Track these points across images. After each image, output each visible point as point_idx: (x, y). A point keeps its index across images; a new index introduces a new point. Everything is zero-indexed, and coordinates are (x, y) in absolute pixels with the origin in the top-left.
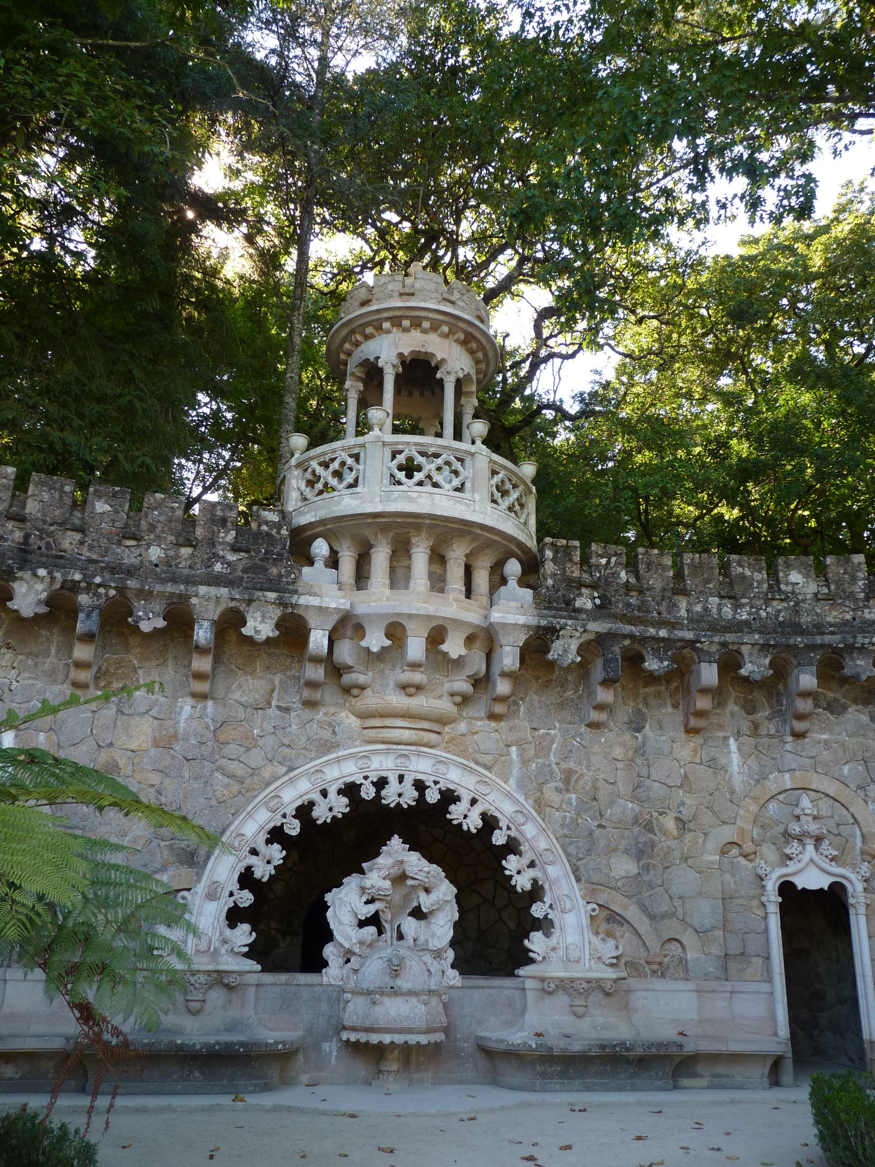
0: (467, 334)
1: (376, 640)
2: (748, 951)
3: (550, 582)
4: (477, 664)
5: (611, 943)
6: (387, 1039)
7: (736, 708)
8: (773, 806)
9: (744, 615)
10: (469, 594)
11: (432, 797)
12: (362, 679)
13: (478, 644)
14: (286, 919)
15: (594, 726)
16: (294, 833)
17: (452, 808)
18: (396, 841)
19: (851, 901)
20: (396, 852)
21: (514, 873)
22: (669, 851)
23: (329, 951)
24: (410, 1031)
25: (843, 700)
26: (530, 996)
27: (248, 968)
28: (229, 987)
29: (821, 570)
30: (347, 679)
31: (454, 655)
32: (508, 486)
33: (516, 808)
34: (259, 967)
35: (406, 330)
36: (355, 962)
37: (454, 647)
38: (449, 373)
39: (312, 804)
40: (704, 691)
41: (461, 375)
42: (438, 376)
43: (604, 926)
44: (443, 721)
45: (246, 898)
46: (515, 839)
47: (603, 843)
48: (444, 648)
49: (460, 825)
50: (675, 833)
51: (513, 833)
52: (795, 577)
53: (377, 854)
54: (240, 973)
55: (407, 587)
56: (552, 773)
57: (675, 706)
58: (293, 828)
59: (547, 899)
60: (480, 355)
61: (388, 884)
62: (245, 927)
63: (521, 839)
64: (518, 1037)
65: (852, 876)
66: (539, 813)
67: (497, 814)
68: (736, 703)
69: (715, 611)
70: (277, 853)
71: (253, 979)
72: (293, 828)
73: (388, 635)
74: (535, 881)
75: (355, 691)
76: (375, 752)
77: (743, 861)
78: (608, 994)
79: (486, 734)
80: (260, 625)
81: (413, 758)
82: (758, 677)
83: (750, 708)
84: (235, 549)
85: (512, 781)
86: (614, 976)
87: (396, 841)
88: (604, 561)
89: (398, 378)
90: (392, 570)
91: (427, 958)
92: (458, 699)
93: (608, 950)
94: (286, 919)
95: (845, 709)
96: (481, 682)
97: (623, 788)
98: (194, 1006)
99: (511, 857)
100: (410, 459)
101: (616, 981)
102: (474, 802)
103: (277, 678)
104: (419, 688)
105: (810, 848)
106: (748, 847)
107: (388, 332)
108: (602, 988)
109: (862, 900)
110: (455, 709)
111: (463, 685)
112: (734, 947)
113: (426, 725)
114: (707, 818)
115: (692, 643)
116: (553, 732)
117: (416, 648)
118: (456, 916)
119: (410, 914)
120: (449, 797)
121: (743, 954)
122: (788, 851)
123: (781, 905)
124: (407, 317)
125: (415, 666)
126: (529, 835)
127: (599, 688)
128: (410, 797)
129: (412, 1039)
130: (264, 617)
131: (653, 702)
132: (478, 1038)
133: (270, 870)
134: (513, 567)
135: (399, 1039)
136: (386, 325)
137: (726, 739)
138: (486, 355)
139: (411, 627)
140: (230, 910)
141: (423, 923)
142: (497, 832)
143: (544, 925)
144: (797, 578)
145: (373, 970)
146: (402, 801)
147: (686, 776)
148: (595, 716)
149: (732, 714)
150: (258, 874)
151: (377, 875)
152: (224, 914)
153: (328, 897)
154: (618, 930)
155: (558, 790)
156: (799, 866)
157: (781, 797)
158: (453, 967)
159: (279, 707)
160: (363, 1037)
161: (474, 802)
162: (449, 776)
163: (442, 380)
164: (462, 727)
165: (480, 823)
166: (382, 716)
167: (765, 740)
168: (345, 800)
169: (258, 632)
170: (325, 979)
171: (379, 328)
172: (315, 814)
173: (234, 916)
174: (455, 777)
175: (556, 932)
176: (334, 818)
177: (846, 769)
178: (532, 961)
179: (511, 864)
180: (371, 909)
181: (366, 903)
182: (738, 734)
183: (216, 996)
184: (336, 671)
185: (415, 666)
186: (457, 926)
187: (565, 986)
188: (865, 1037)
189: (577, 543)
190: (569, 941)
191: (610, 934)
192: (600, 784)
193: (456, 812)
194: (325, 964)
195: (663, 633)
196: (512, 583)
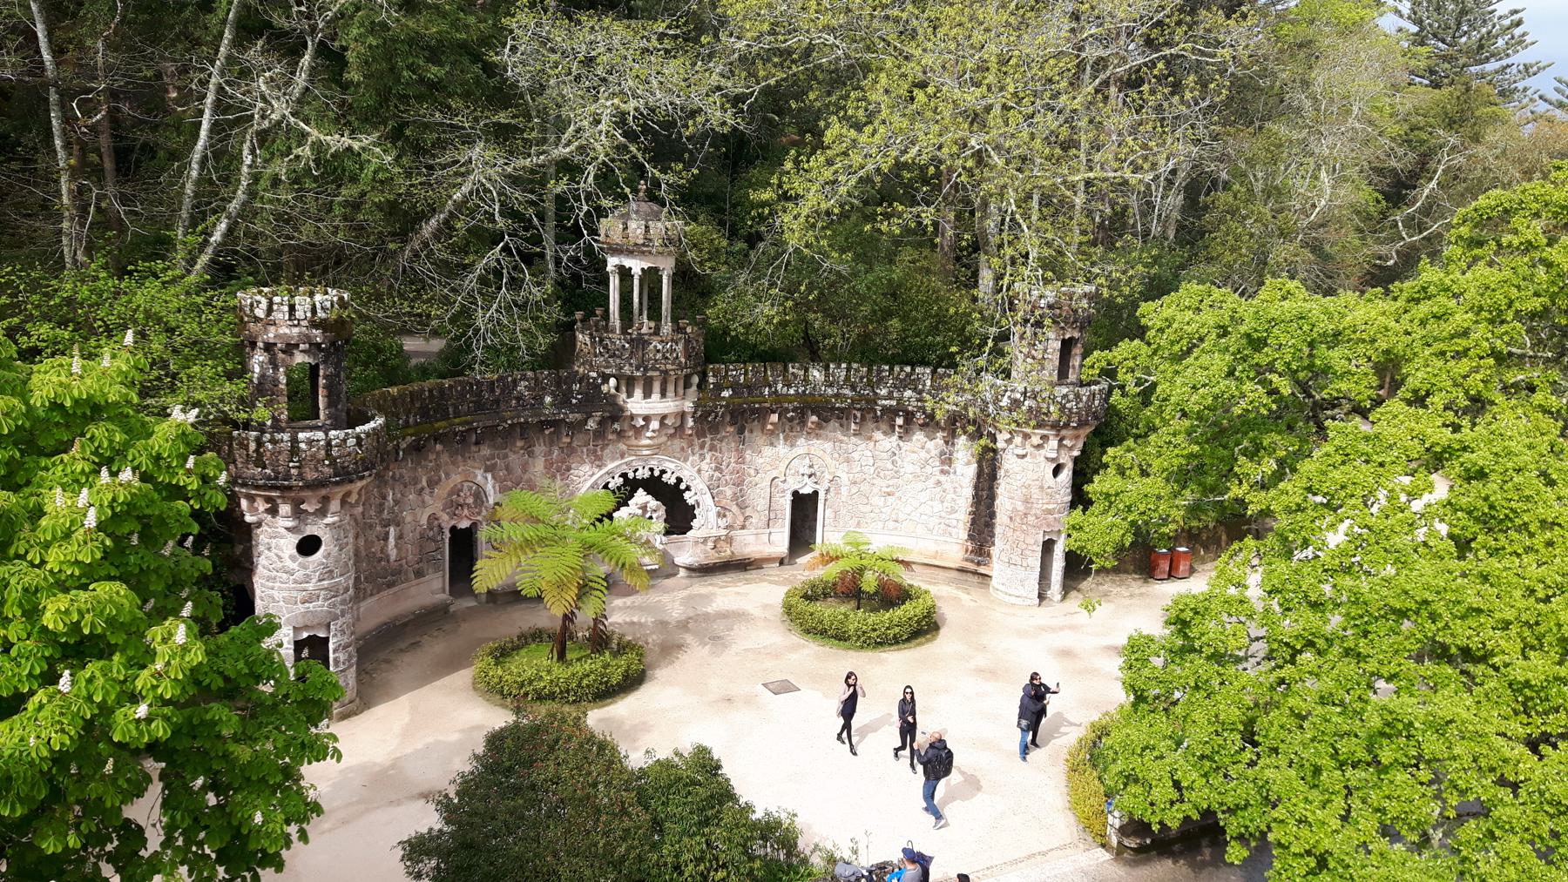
11: (657, 473)
20: (641, 496)
37: (668, 422)
52: (816, 373)
79: (678, 443)
117: (655, 425)
128: (647, 474)
134: (696, 379)
144: (816, 374)
179: (687, 495)
190: (706, 522)
193: (665, 478)
196: (694, 388)
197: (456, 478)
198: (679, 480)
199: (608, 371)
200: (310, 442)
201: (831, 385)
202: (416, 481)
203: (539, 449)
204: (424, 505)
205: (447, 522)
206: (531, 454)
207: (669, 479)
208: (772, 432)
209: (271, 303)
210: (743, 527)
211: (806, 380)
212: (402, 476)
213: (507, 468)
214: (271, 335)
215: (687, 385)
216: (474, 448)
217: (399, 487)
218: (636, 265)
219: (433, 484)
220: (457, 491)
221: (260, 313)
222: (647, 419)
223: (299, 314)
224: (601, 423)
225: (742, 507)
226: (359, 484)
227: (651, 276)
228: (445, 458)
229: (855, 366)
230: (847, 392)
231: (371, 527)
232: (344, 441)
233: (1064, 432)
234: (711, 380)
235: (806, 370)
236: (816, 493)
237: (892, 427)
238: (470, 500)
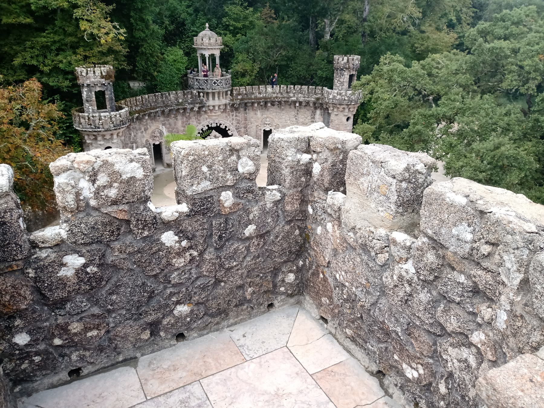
1: (211, 108)
11: (218, 125)
37: (221, 107)
79: (224, 115)
97: (243, 119)
117: (217, 108)
120: (220, 124)
128: (215, 125)
134: (229, 92)
144: (269, 89)
174: (221, 122)
196: (229, 95)
197: (153, 128)
198: (226, 127)
199: (200, 91)
200: (105, 117)
201: (274, 93)
202: (140, 129)
203: (179, 117)
204: (144, 137)
205: (152, 143)
206: (177, 119)
207: (223, 127)
208: (256, 110)
209: (87, 71)
211: (266, 92)
212: (135, 127)
213: (170, 124)
214: (88, 82)
215: (226, 94)
216: (158, 118)
217: (135, 131)
218: (207, 54)
219: (146, 130)
220: (154, 132)
221: (84, 74)
222: (214, 106)
223: (97, 74)
224: (199, 108)
226: (122, 130)
227: (212, 57)
228: (149, 121)
229: (282, 86)
230: (279, 95)
231: (127, 144)
232: (116, 116)
233: (350, 106)
234: (234, 92)
235: (266, 88)
236: (271, 130)
237: (295, 107)
238: (158, 135)
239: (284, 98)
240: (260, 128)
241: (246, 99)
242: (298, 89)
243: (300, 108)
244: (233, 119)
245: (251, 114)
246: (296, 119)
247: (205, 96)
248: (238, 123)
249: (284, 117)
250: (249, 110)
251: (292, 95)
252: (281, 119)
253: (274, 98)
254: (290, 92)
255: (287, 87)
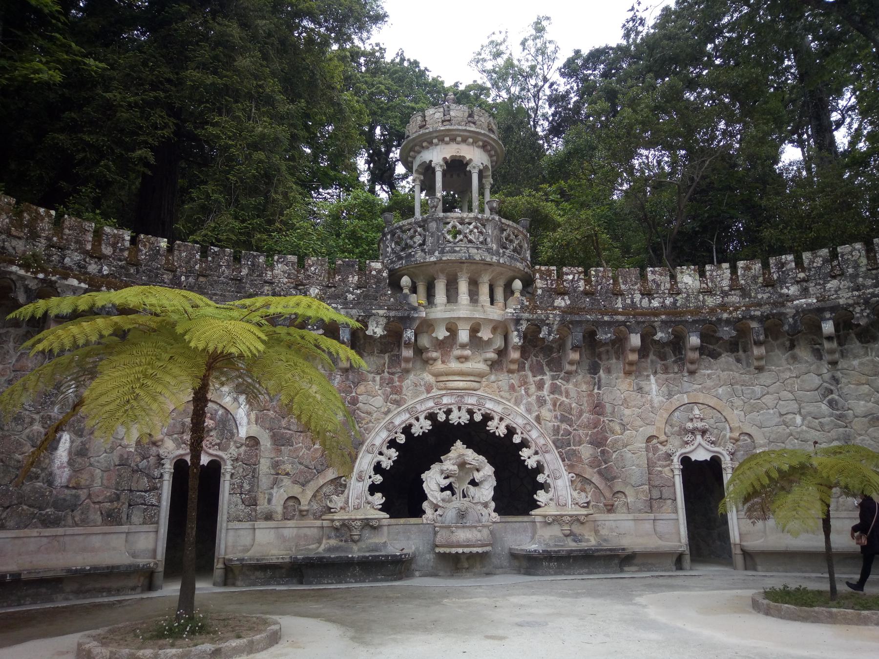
0: (484, 142)
1: (442, 333)
2: (663, 497)
3: (540, 292)
4: (499, 343)
5: (583, 494)
6: (460, 550)
7: (654, 358)
8: (677, 414)
9: (655, 303)
10: (492, 303)
11: (478, 418)
12: (434, 355)
13: (499, 331)
14: (401, 491)
15: (569, 373)
16: (402, 442)
17: (490, 423)
18: (459, 443)
19: (723, 466)
21: (526, 458)
22: (616, 441)
23: (425, 505)
24: (474, 546)
25: (719, 350)
26: (538, 524)
27: (382, 517)
28: (374, 528)
29: (702, 274)
30: (424, 355)
31: (485, 338)
32: (512, 237)
33: (525, 422)
34: (388, 516)
35: (447, 143)
36: (439, 512)
37: (485, 334)
38: (474, 167)
39: (411, 426)
40: (633, 350)
41: (481, 167)
42: (468, 169)
43: (579, 485)
44: (481, 375)
45: (379, 479)
46: (526, 439)
47: (577, 439)
48: (479, 335)
49: (494, 433)
50: (619, 432)
51: (525, 436)
53: (449, 451)
54: (379, 519)
55: (456, 301)
56: (545, 401)
57: (618, 358)
58: (402, 439)
59: (546, 472)
60: (493, 153)
61: (456, 467)
62: (379, 495)
63: (529, 439)
64: (533, 547)
65: (724, 453)
66: (539, 423)
67: (515, 426)
68: (654, 355)
69: (638, 302)
70: (393, 453)
71: (385, 522)
72: (402, 439)
73: (448, 330)
74: (538, 462)
75: (431, 362)
76: (443, 395)
77: (660, 446)
78: (582, 523)
80: (376, 329)
81: (466, 398)
82: (665, 340)
83: (663, 357)
84: (358, 288)
85: (522, 407)
86: (585, 513)
87: (459, 443)
88: (570, 277)
89: (444, 174)
90: (448, 290)
91: (480, 507)
92: (490, 363)
93: (582, 498)
94: (401, 491)
95: (720, 355)
96: (502, 353)
98: (356, 537)
99: (524, 449)
100: (454, 227)
101: (587, 515)
102: (501, 419)
103: (386, 356)
104: (466, 359)
105: (699, 437)
106: (663, 438)
107: (437, 145)
108: (578, 520)
109: (730, 465)
110: (488, 368)
111: (492, 355)
112: (656, 494)
113: (472, 378)
114: (639, 422)
115: (624, 323)
116: (545, 377)
117: (464, 336)
118: (495, 484)
119: (469, 484)
120: (487, 418)
121: (661, 498)
122: (686, 439)
123: (683, 470)
124: (447, 136)
125: (463, 346)
126: (534, 437)
127: (570, 352)
128: (465, 419)
129: (474, 550)
130: (377, 324)
131: (604, 357)
132: (510, 549)
133: (390, 463)
134: (518, 284)
135: (467, 550)
136: (435, 141)
137: (648, 376)
138: (496, 152)
139: (461, 325)
140: (370, 486)
141: (476, 488)
142: (515, 436)
143: (544, 487)
144: (688, 279)
145: (451, 514)
146: (461, 421)
147: (625, 399)
148: (568, 367)
149: (652, 361)
150: (384, 465)
151: (449, 463)
152: (367, 489)
153: (423, 476)
154: (588, 487)
155: (550, 411)
156: (693, 447)
157: (682, 408)
158: (495, 511)
159: (388, 373)
160: (447, 550)
161: (501, 419)
162: (487, 406)
163: (470, 171)
164: (493, 378)
165: (506, 431)
166: (447, 375)
167: (672, 375)
168: (429, 422)
169: (375, 333)
170: (425, 521)
171: (431, 143)
172: (413, 431)
173: (373, 489)
175: (552, 490)
176: (424, 432)
177: (720, 390)
178: (539, 507)
179: (525, 453)
180: (446, 483)
181: (445, 478)
182: (655, 373)
183: (367, 533)
184: (419, 351)
185: (463, 346)
186: (495, 489)
187: (557, 520)
188: (732, 541)
189: (554, 268)
191: (583, 490)
192: (574, 405)
193: (492, 426)
194: (424, 512)
195: (606, 318)
196: (517, 294)
201: (709, 292)
210: (610, 509)
225: (608, 476)
234: (539, 283)
235: (673, 277)
239: (759, 305)
240: (663, 449)
241: (590, 311)
242: (819, 262)
243: (843, 355)
244: (541, 402)
245: (618, 388)
246: (831, 403)
247: (422, 289)
248: (563, 419)
249: (769, 400)
250: (609, 371)
251: (793, 290)
252: (754, 409)
253: (712, 311)
254: (782, 282)
255: (766, 266)
